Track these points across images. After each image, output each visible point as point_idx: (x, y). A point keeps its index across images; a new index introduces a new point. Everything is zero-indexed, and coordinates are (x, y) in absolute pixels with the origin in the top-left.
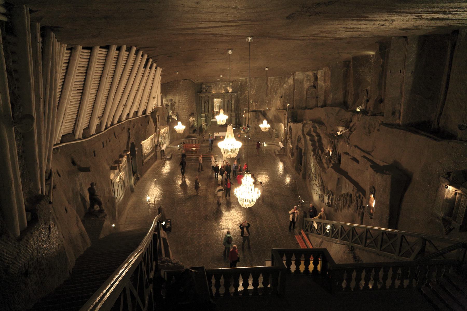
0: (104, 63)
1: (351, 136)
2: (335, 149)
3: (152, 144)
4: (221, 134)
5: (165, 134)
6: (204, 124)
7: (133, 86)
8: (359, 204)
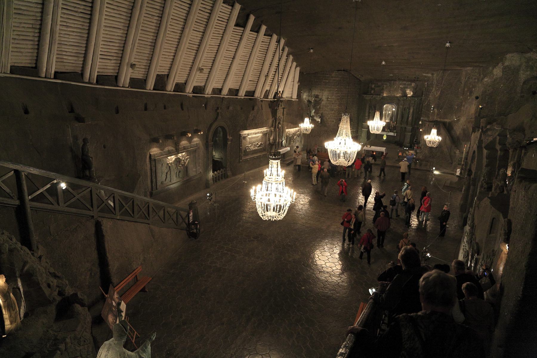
5: (295, 137)
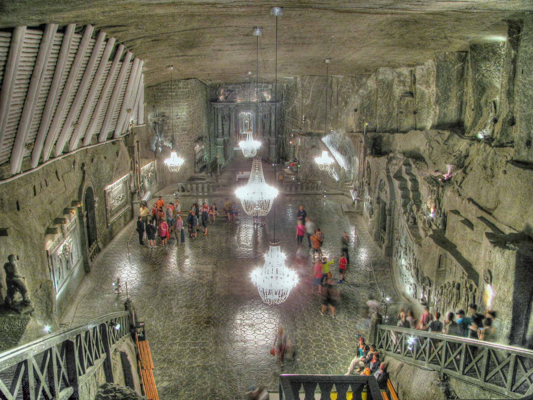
0: (36, 55)
1: (464, 182)
2: (439, 203)
3: (125, 190)
4: (246, 173)
6: (220, 156)
7: (90, 92)
8: (470, 300)
